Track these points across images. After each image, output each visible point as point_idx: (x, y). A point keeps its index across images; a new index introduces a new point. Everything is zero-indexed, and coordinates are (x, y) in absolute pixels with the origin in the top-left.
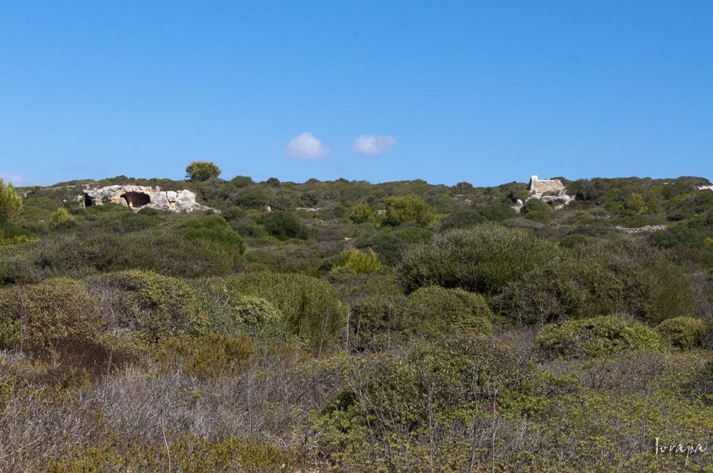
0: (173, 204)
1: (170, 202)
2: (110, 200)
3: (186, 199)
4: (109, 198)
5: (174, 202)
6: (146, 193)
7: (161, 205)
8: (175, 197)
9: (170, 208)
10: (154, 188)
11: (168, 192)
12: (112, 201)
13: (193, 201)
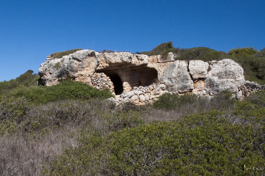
0: (202, 84)
1: (194, 80)
2: (74, 78)
3: (227, 74)
4: (72, 74)
5: (203, 79)
6: (150, 65)
7: (176, 86)
8: (205, 70)
9: (195, 92)
10: (165, 57)
11: (192, 62)
12: (77, 80)
13: (241, 78)
